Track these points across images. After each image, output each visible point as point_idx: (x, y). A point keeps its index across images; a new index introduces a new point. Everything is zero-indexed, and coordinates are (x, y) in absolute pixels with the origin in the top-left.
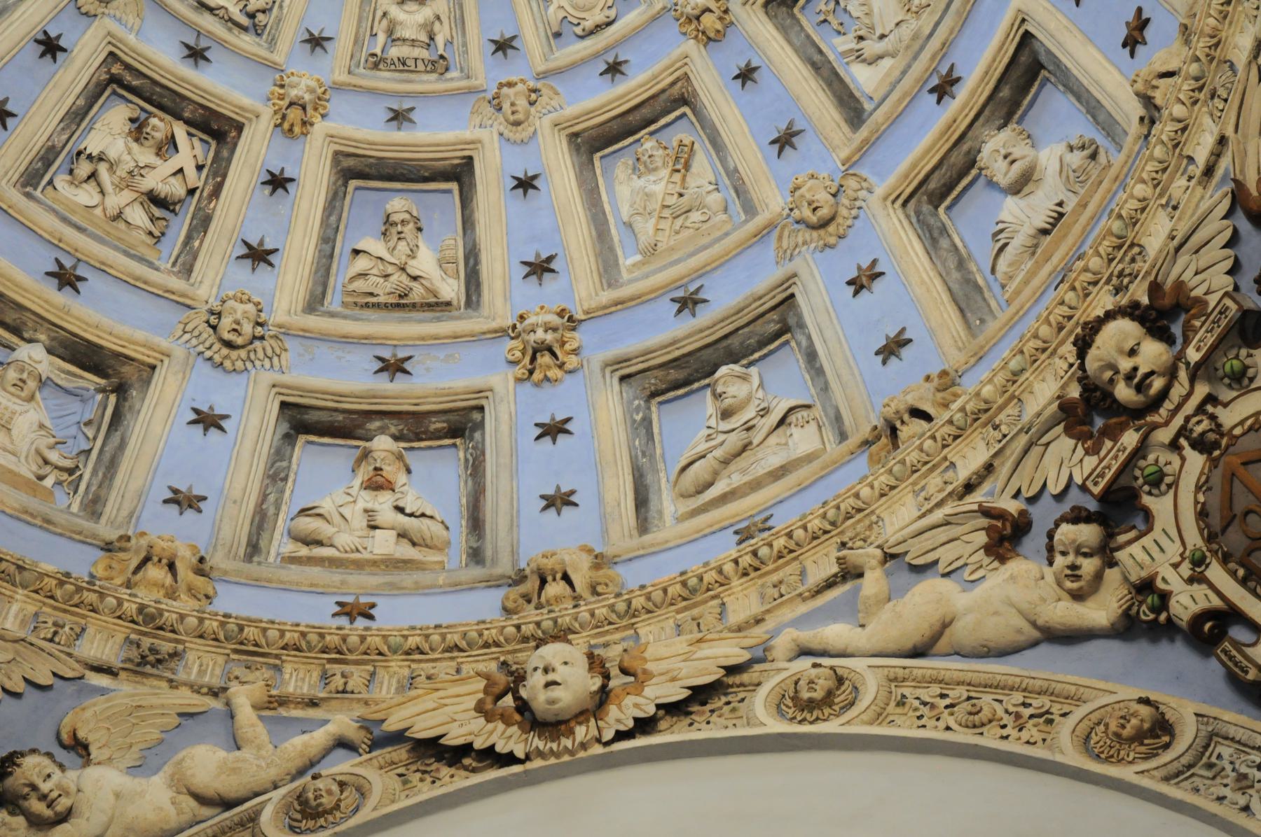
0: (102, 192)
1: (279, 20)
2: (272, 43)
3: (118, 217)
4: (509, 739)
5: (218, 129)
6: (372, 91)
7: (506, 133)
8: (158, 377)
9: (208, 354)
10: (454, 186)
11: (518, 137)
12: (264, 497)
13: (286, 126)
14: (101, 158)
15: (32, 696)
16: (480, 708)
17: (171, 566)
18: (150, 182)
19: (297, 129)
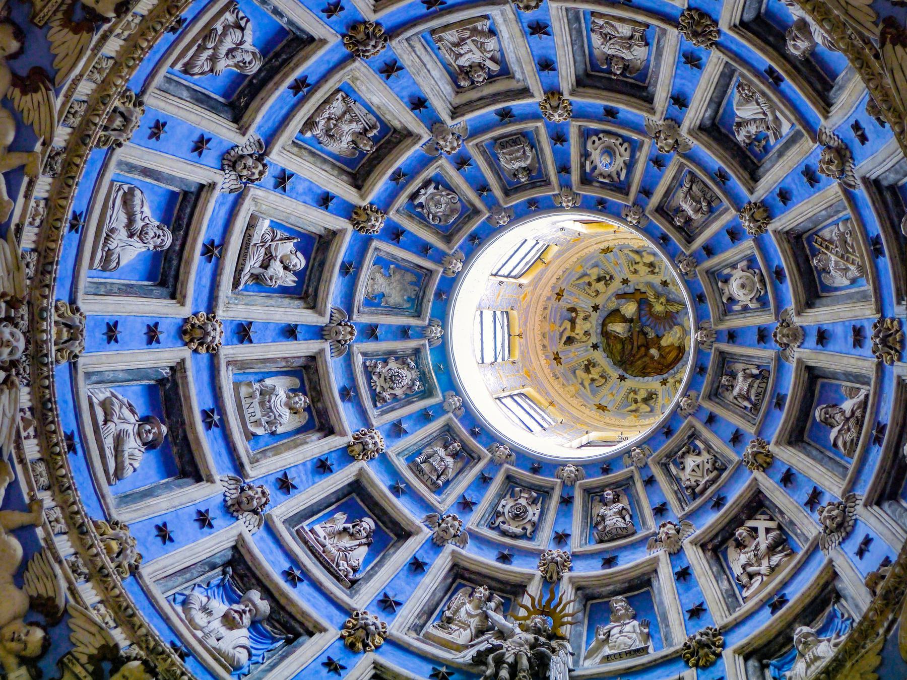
0: (759, 574)
1: (722, 455)
2: (730, 462)
3: (772, 569)
5: (757, 504)
6: (767, 414)
7: (798, 344)
8: (838, 570)
9: (841, 539)
10: (820, 381)
11: (801, 337)
13: (765, 465)
14: (744, 567)
18: (763, 547)
19: (768, 460)
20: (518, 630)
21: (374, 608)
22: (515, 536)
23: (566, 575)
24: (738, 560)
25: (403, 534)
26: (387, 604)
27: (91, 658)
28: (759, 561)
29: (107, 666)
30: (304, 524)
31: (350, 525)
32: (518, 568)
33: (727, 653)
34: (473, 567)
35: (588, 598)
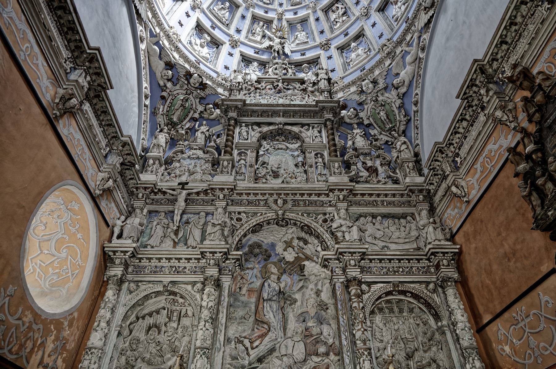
4: (431, 13)
12: (387, 23)
15: (387, 76)
16: (425, 14)
17: (385, 45)
18: (341, 13)
20: (275, 38)
21: (235, 33)
22: (268, 4)
23: (284, 17)
24: (333, 16)
25: (238, 7)
26: (238, 31)
27: (184, 75)
28: (339, 18)
29: (188, 77)
30: (211, 7)
31: (223, 6)
32: (271, 15)
33: (332, 47)
34: (258, 16)
35: (290, 24)
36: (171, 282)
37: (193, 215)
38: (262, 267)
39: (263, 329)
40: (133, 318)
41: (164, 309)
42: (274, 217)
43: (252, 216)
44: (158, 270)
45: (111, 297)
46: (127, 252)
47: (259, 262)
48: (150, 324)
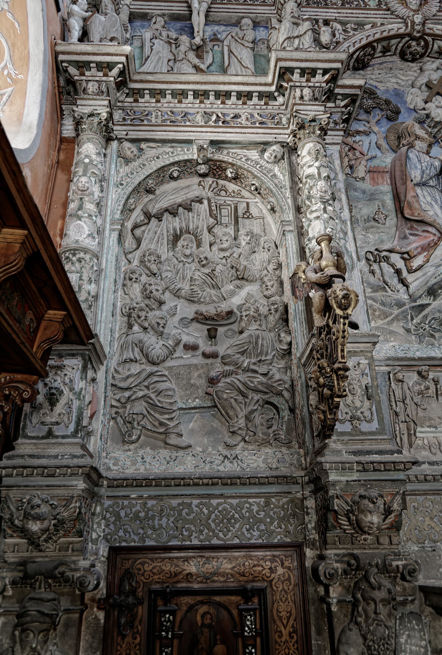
36: (213, 143)
37: (223, 28)
38: (388, 131)
39: (426, 234)
40: (137, 215)
41: (200, 201)
42: (402, 31)
43: (355, 30)
44: (179, 118)
45: (94, 157)
46: (110, 66)
47: (378, 122)
48: (175, 230)
